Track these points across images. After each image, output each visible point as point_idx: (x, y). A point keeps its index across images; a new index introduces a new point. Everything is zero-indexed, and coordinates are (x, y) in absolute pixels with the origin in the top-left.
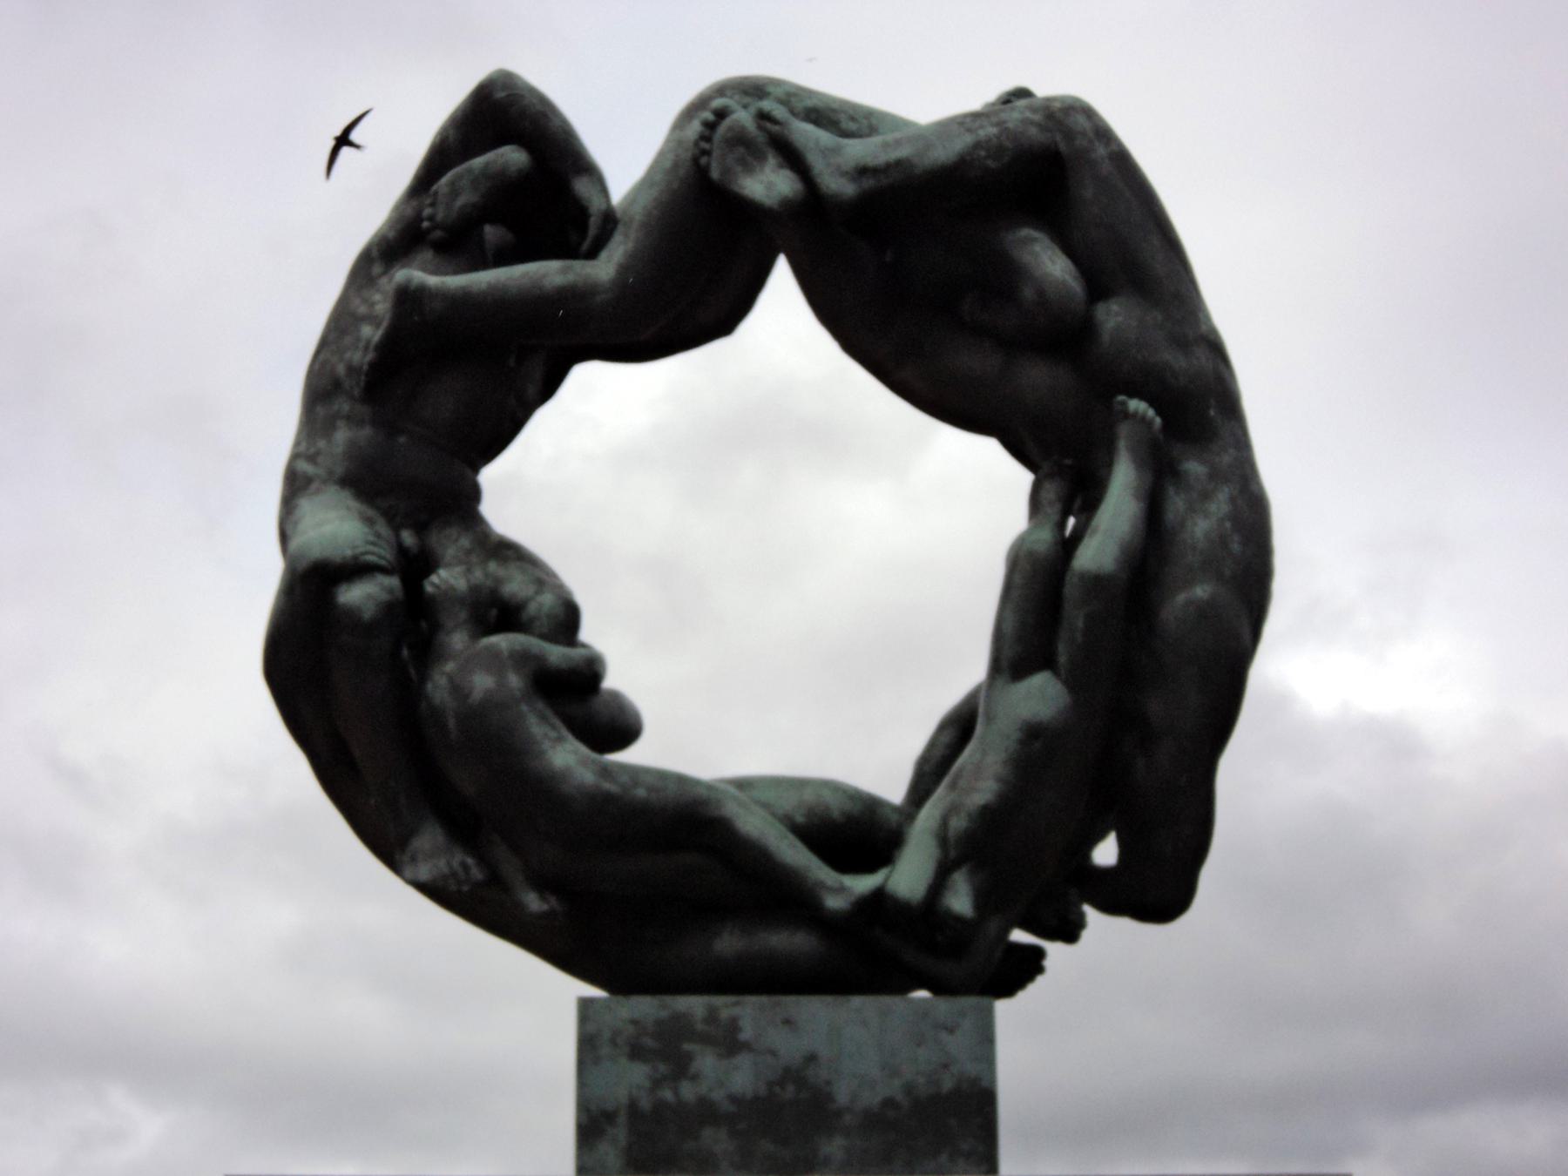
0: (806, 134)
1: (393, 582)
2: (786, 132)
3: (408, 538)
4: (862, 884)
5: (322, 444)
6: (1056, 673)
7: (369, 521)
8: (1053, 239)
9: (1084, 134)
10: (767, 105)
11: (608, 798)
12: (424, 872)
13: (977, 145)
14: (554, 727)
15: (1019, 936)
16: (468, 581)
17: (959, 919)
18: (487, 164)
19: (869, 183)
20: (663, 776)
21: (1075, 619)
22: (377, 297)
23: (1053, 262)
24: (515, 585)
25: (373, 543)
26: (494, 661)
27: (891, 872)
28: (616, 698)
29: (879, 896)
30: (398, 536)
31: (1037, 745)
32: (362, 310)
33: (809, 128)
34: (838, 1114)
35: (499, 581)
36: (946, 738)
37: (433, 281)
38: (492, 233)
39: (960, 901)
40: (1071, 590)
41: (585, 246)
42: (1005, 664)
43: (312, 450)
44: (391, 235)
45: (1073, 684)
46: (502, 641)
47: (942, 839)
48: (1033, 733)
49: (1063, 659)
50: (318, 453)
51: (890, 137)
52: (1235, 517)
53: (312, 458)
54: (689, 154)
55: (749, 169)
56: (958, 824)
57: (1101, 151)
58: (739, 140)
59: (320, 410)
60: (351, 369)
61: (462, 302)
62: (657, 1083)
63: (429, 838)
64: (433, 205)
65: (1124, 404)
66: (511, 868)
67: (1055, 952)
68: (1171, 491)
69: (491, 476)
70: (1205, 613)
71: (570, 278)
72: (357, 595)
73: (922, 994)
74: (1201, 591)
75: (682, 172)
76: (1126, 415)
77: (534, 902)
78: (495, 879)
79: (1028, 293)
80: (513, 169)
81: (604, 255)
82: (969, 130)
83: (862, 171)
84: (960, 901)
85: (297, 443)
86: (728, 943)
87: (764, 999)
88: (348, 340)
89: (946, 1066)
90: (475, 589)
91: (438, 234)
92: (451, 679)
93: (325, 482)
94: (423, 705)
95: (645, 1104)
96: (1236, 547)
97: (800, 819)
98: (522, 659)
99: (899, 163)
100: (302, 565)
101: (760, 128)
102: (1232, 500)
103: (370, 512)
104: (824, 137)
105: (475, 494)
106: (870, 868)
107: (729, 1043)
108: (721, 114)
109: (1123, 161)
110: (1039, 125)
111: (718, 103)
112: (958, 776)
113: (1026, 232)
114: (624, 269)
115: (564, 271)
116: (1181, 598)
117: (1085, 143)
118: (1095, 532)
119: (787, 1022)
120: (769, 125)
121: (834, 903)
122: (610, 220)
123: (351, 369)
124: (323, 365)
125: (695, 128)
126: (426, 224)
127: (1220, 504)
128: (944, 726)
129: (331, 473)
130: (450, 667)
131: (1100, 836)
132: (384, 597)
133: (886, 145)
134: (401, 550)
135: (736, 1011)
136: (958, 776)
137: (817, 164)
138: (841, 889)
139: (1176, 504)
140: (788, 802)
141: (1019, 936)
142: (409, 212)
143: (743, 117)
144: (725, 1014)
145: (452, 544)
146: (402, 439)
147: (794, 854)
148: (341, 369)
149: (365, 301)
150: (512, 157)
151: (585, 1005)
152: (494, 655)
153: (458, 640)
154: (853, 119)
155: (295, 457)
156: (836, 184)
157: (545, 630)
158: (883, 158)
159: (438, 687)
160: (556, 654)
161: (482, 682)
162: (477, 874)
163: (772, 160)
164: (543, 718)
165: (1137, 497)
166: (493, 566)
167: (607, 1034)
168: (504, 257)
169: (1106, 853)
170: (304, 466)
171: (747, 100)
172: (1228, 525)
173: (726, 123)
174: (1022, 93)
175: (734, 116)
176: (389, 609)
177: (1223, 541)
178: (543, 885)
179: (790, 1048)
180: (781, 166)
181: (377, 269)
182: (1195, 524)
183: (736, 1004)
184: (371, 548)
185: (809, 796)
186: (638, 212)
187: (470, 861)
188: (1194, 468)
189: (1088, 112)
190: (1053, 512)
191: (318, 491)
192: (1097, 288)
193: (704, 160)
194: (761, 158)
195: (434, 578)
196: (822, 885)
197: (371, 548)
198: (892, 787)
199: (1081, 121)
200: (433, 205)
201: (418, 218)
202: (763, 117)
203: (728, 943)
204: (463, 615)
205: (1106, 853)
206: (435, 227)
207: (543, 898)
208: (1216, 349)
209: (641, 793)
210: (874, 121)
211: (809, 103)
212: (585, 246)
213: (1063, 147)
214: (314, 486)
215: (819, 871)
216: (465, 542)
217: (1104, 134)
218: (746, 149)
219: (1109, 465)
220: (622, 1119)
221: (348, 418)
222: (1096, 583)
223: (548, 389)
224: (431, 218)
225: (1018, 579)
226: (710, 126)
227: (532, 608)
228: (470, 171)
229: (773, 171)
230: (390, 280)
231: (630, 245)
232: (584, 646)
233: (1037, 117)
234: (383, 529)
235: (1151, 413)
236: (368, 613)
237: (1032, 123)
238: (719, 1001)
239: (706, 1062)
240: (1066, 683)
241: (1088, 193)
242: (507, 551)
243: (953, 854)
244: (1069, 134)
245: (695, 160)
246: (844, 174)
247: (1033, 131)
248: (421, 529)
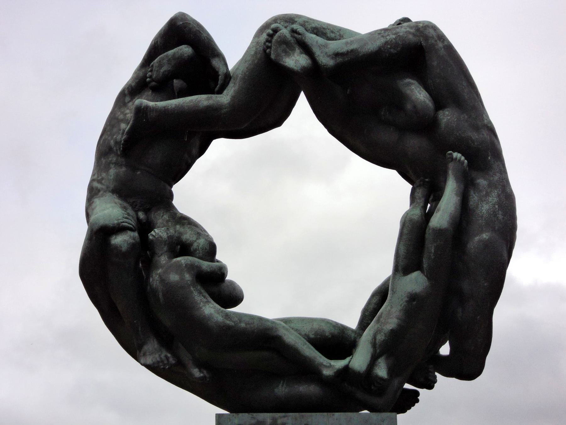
0: (312, 39)
1: (136, 234)
2: (303, 38)
3: (141, 215)
4: (339, 364)
5: (104, 175)
6: (423, 272)
7: (125, 208)
8: (419, 83)
9: (433, 37)
10: (295, 26)
11: (229, 328)
12: (149, 360)
13: (386, 43)
14: (205, 297)
15: (407, 386)
16: (167, 234)
17: (382, 379)
18: (175, 53)
19: (339, 60)
20: (252, 317)
21: (431, 248)
22: (128, 111)
23: (420, 94)
24: (188, 235)
25: (126, 218)
26: (178, 268)
27: (351, 358)
28: (232, 283)
29: (347, 369)
30: (137, 214)
31: (415, 303)
32: (121, 117)
33: (314, 36)
35: (181, 234)
36: (375, 300)
37: (151, 104)
38: (177, 83)
39: (382, 371)
40: (429, 236)
41: (217, 89)
42: (400, 268)
43: (100, 178)
44: (133, 84)
45: (429, 277)
46: (182, 260)
47: (374, 344)
48: (413, 298)
49: (425, 265)
50: (102, 179)
51: (349, 40)
52: (500, 204)
53: (100, 181)
54: (262, 49)
55: (287, 54)
56: (380, 338)
57: (440, 45)
58: (284, 42)
59: (103, 160)
60: (117, 143)
61: (165, 113)
63: (152, 345)
64: (151, 71)
65: (451, 154)
66: (186, 358)
67: (423, 392)
68: (472, 192)
69: (176, 188)
70: (487, 245)
71: (211, 102)
73: (366, 411)
74: (485, 236)
75: (259, 56)
76: (452, 159)
77: (197, 373)
78: (180, 363)
79: (409, 107)
80: (186, 55)
81: (225, 92)
82: (383, 36)
83: (337, 55)
84: (382, 371)
85: (93, 175)
87: (297, 414)
88: (115, 130)
90: (170, 237)
91: (153, 83)
92: (160, 276)
93: (105, 192)
94: (149, 288)
96: (500, 217)
97: (312, 336)
98: (191, 267)
99: (352, 51)
100: (96, 228)
101: (292, 36)
102: (499, 196)
103: (125, 204)
104: (320, 40)
105: (171, 196)
106: (343, 358)
108: (275, 31)
109: (450, 49)
110: (414, 35)
111: (273, 26)
112: (381, 316)
113: (408, 80)
114: (233, 97)
115: (208, 99)
116: (477, 238)
117: (433, 42)
118: (438, 210)
120: (296, 35)
121: (327, 372)
122: (228, 77)
123: (117, 143)
124: (105, 140)
125: (264, 36)
126: (148, 79)
127: (493, 198)
128: (373, 295)
129: (108, 187)
130: (160, 271)
131: (443, 343)
132: (132, 241)
133: (347, 43)
134: (138, 220)
135: (285, 420)
136: (381, 316)
137: (317, 52)
138: (330, 366)
139: (474, 198)
140: (306, 329)
141: (407, 386)
142: (141, 74)
143: (285, 32)
144: (279, 421)
146: (139, 173)
147: (310, 351)
148: (112, 142)
149: (122, 113)
150: (185, 50)
151: (219, 416)
152: (179, 265)
153: (163, 259)
154: (332, 32)
155: (92, 181)
156: (325, 60)
157: (201, 255)
158: (345, 49)
159: (155, 279)
160: (206, 265)
161: (174, 277)
162: (172, 361)
163: (298, 51)
164: (200, 293)
165: (457, 195)
166: (178, 227)
168: (183, 93)
169: (445, 350)
170: (96, 184)
171: (287, 24)
172: (497, 206)
173: (278, 34)
174: (406, 20)
175: (281, 31)
176: (133, 246)
177: (495, 214)
178: (200, 365)
180: (301, 53)
181: (127, 99)
182: (482, 206)
183: (284, 417)
184: (125, 220)
185: (316, 326)
186: (240, 73)
187: (169, 355)
188: (482, 182)
189: (435, 28)
190: (421, 202)
191: (102, 196)
192: (439, 105)
193: (268, 51)
194: (293, 50)
195: (153, 233)
196: (322, 364)
197: (125, 220)
199: (431, 31)
200: (151, 71)
201: (145, 77)
202: (293, 31)
204: (165, 248)
205: (445, 350)
206: (153, 80)
207: (200, 371)
208: (492, 130)
209: (243, 325)
210: (342, 33)
211: (313, 25)
212: (217, 89)
213: (424, 44)
214: (101, 193)
215: (320, 358)
216: (166, 217)
217: (442, 37)
219: (445, 182)
221: (116, 164)
222: (439, 232)
223: (202, 150)
224: (150, 77)
225: (405, 231)
226: (271, 36)
227: (195, 245)
228: (167, 56)
229: (298, 56)
230: (133, 104)
231: (237, 87)
232: (218, 261)
233: (412, 31)
234: (130, 211)
235: (463, 158)
236: (124, 249)
237: (410, 33)
238: (277, 415)
240: (426, 276)
241: (435, 63)
242: (184, 221)
243: (378, 351)
244: (427, 38)
245: (265, 51)
246: (329, 56)
247: (411, 37)
248: (147, 211)
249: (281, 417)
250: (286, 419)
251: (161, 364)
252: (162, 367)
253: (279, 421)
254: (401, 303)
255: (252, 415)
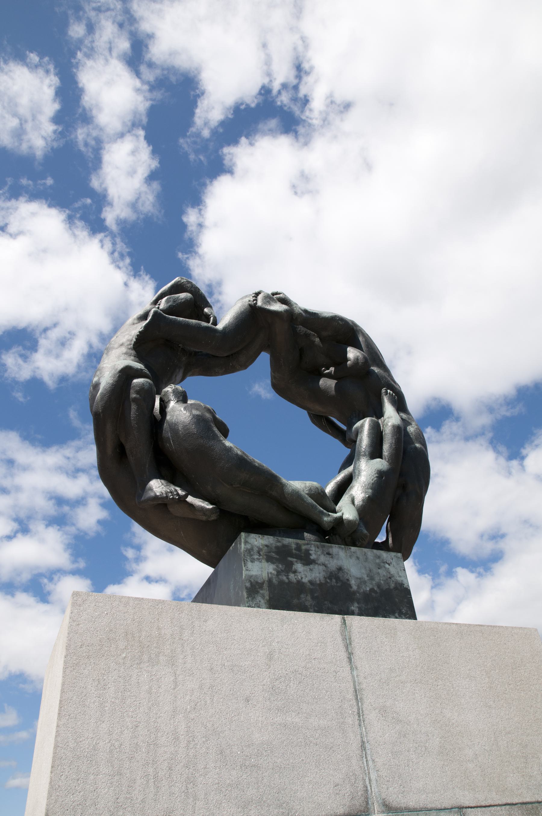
34: (354, 593)
62: (279, 573)
89: (390, 578)
95: (275, 581)
107: (307, 561)
119: (328, 554)
144: (304, 547)
167: (256, 549)
179: (333, 564)
220: (265, 586)
239: (299, 567)
249: (305, 544)
250: (309, 546)
251: (170, 494)
252: (171, 497)
253: (304, 547)
254: (373, 478)
255: (277, 539)
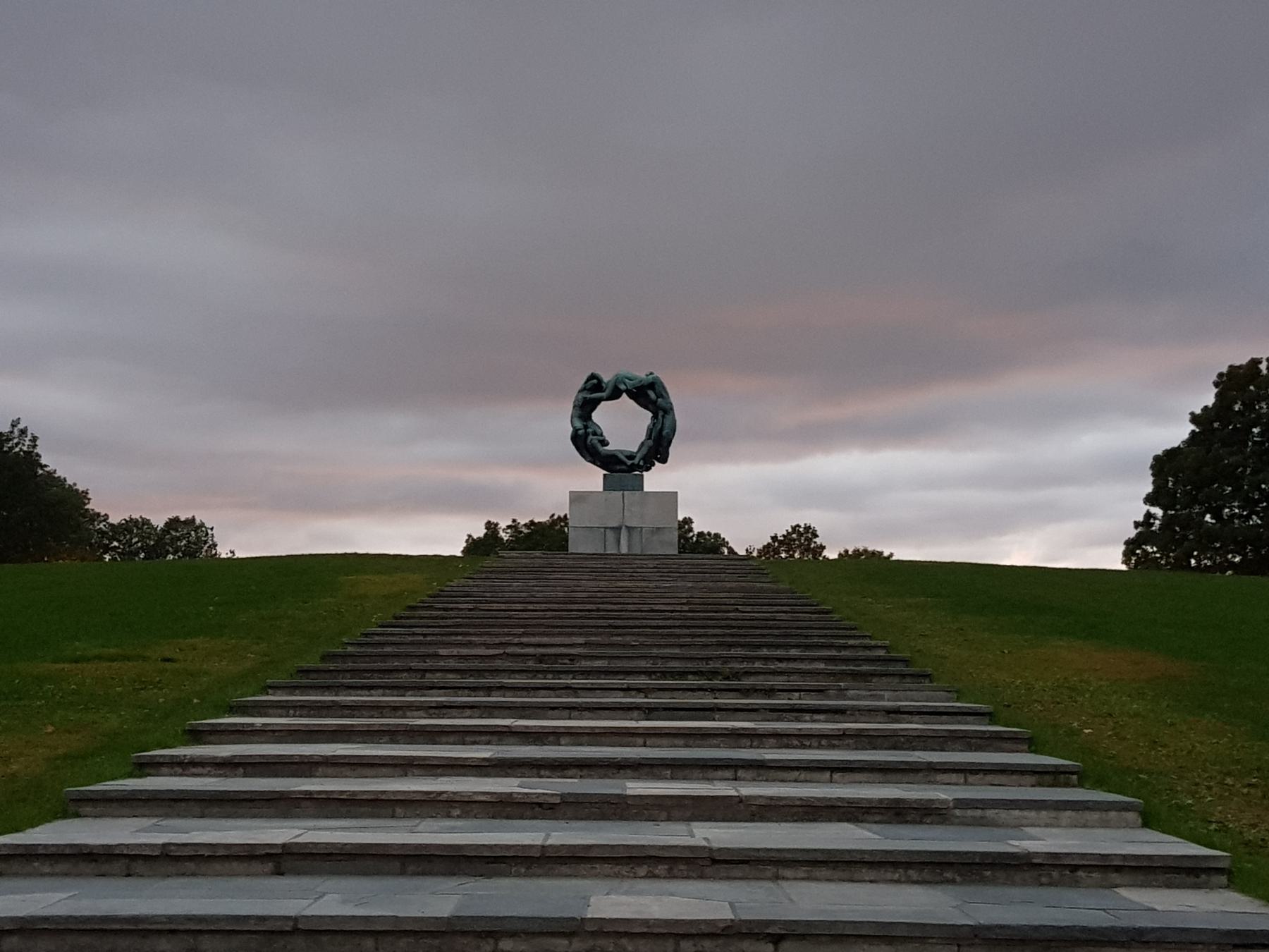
39: (641, 463)
46: (595, 437)
63: (587, 456)
72: (581, 432)
77: (598, 464)
86: (618, 467)
134: (584, 425)
137: (627, 384)
140: (626, 454)
145: (590, 423)
150: (595, 381)
151: (605, 475)
160: (601, 438)
178: (600, 461)
192: (658, 397)
198: (635, 449)
203: (618, 467)
218: (620, 383)
